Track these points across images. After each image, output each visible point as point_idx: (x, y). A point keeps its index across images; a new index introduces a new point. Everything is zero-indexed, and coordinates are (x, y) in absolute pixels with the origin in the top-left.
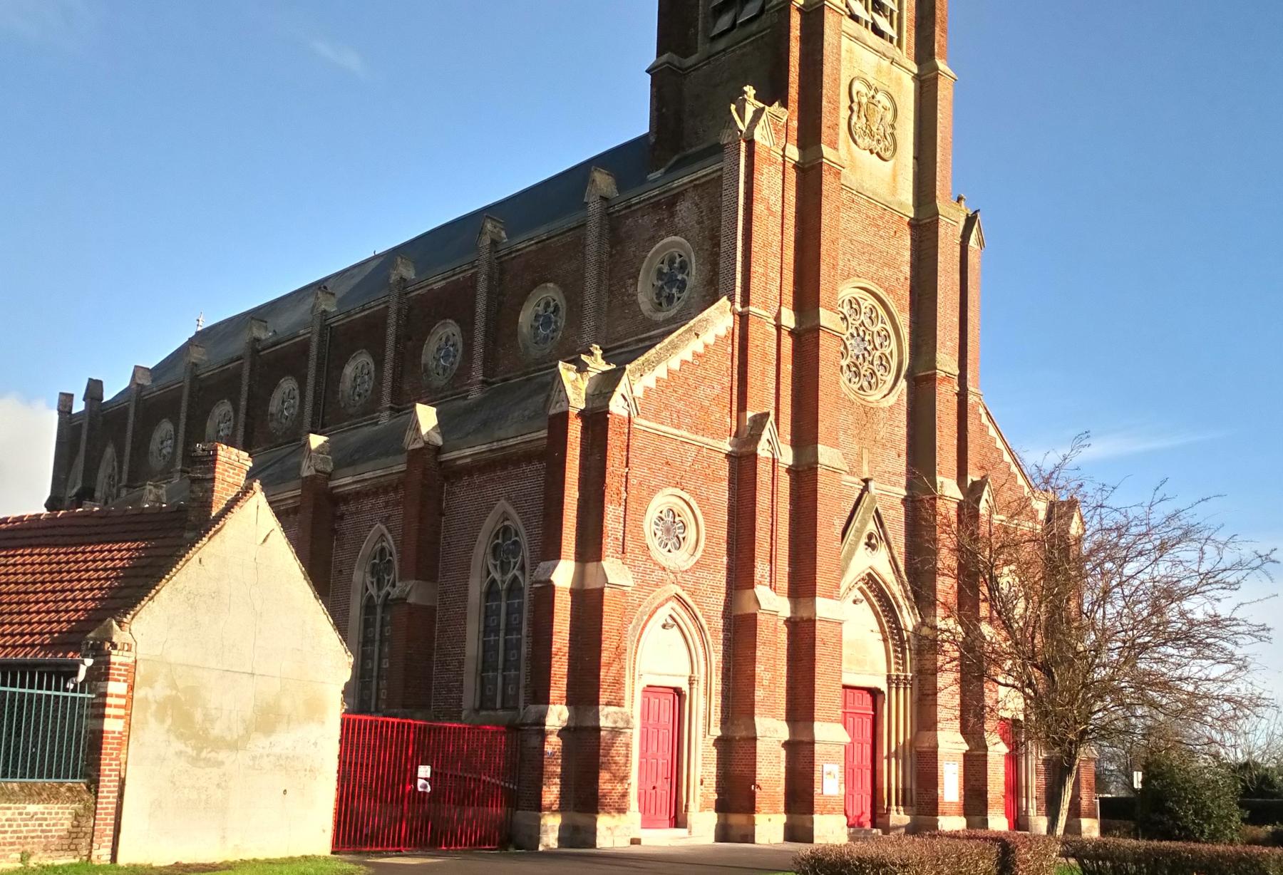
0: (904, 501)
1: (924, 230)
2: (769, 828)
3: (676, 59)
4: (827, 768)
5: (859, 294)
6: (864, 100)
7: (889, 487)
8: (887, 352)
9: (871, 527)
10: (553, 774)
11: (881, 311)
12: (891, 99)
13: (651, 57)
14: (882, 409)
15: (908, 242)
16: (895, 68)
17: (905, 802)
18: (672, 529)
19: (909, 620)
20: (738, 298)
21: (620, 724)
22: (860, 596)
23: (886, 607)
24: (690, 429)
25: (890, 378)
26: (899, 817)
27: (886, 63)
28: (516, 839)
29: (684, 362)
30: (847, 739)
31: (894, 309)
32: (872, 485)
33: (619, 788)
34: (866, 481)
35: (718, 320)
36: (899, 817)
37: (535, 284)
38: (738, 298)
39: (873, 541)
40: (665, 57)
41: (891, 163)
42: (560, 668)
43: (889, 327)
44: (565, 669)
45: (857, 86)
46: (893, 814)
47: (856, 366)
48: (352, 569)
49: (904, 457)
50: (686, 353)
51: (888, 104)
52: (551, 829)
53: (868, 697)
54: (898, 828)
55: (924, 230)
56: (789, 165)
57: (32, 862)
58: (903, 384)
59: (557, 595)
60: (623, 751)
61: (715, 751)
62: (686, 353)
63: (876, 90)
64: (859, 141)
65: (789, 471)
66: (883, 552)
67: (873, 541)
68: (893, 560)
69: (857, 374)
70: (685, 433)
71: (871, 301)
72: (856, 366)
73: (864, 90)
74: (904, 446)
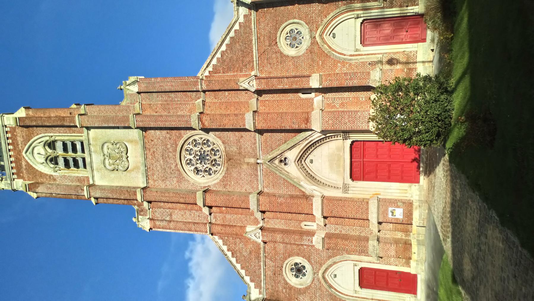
5: (184, 162)
7: (258, 144)
8: (200, 141)
9: (277, 162)
11: (186, 146)
14: (225, 148)
16: (91, 142)
18: (299, 270)
19: (317, 136)
22: (308, 161)
23: (313, 145)
24: (259, 261)
27: (91, 147)
31: (182, 142)
32: (259, 161)
39: (283, 159)
43: (190, 140)
47: (212, 161)
58: (211, 133)
63: (104, 155)
64: (126, 166)
66: (287, 154)
67: (283, 159)
68: (290, 149)
70: (262, 264)
72: (212, 161)
73: (107, 162)
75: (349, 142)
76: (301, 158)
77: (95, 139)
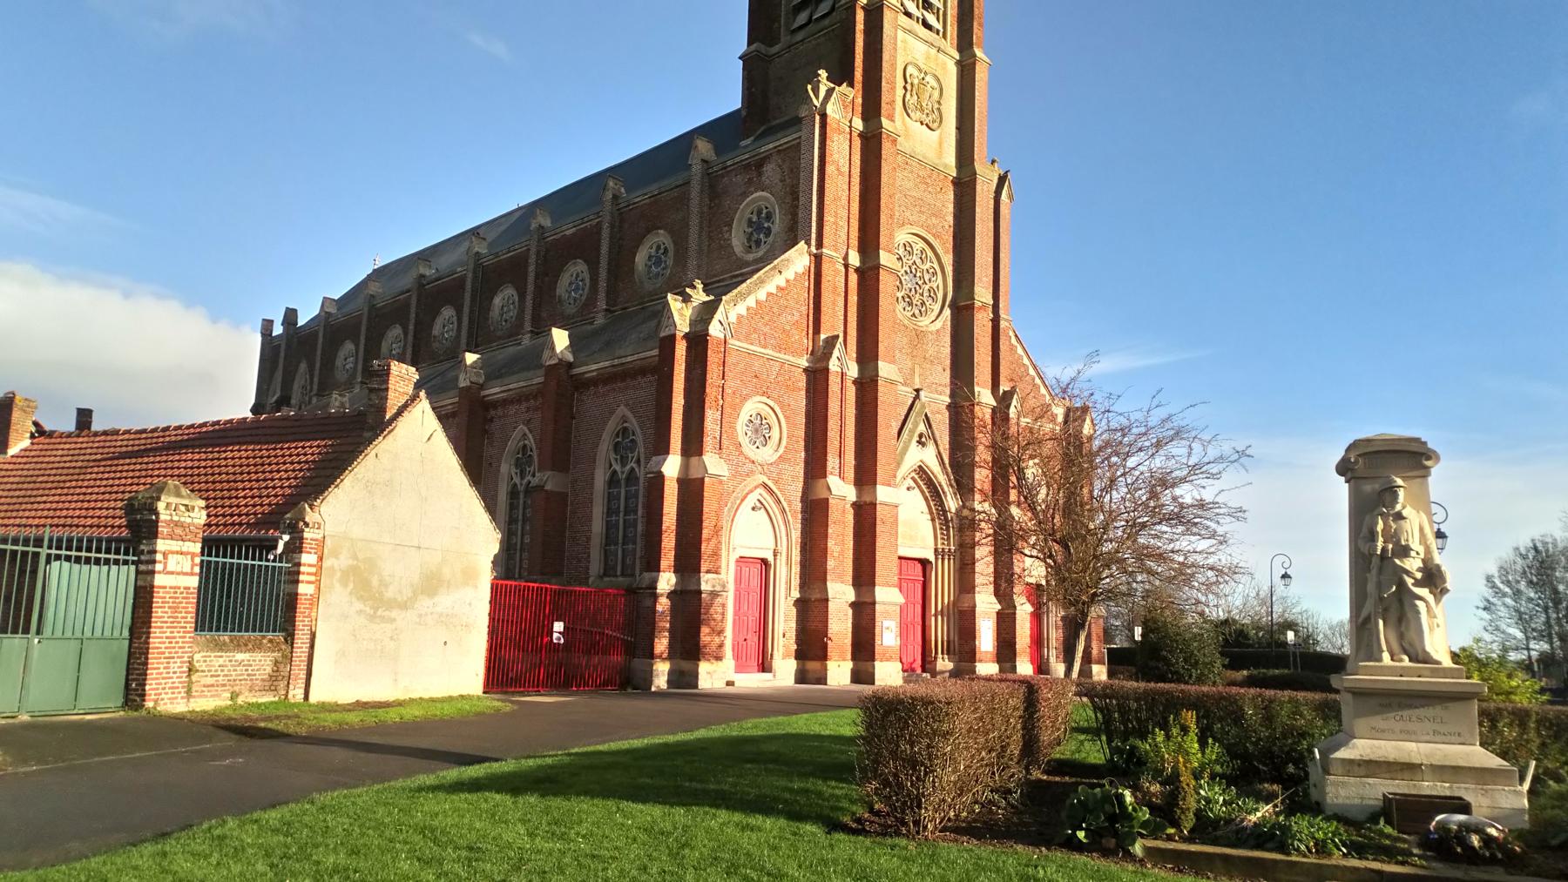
0: (949, 407)
1: (964, 187)
2: (839, 672)
3: (763, 48)
4: (886, 623)
6: (916, 81)
9: (922, 428)
10: (663, 629)
11: (930, 253)
12: (938, 80)
13: (743, 46)
15: (952, 197)
16: (941, 56)
17: (949, 651)
18: (760, 430)
19: (952, 504)
20: (813, 242)
21: (718, 588)
23: (934, 493)
24: (774, 348)
25: (937, 307)
26: (944, 664)
27: (934, 51)
28: (633, 682)
29: (769, 294)
30: (902, 600)
31: (940, 251)
32: (922, 393)
33: (717, 640)
34: (917, 391)
35: (798, 260)
36: (944, 664)
37: (648, 231)
38: (813, 242)
40: (754, 47)
41: (937, 133)
42: (669, 542)
43: (936, 266)
44: (673, 544)
45: (910, 70)
46: (940, 661)
48: (500, 462)
49: (948, 371)
50: (771, 287)
51: (935, 84)
52: (661, 673)
53: (919, 566)
54: (943, 672)
55: (964, 187)
56: (855, 134)
57: (240, 701)
58: (947, 312)
59: (667, 483)
60: (720, 610)
61: (794, 610)
62: (771, 287)
65: (855, 382)
66: (930, 450)
69: (910, 304)
71: (922, 244)
73: (916, 73)
74: (948, 362)
75: (932, 558)
76: (922, 471)
77: (944, 68)
